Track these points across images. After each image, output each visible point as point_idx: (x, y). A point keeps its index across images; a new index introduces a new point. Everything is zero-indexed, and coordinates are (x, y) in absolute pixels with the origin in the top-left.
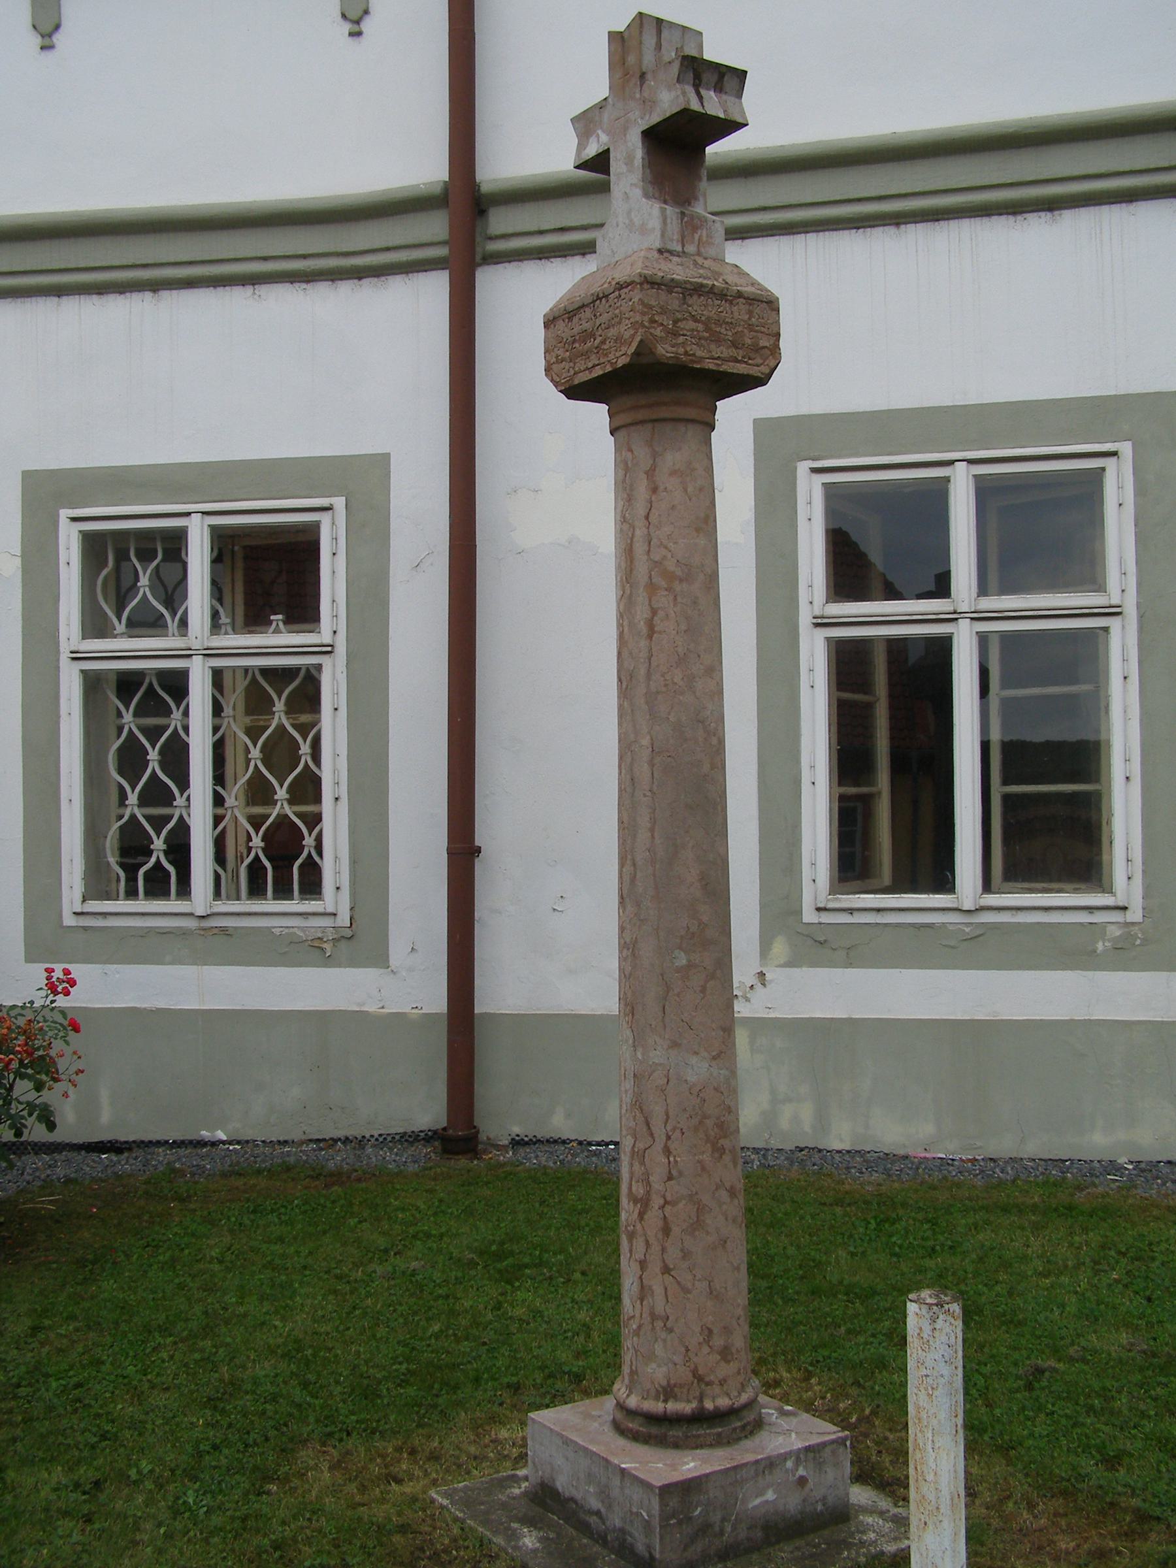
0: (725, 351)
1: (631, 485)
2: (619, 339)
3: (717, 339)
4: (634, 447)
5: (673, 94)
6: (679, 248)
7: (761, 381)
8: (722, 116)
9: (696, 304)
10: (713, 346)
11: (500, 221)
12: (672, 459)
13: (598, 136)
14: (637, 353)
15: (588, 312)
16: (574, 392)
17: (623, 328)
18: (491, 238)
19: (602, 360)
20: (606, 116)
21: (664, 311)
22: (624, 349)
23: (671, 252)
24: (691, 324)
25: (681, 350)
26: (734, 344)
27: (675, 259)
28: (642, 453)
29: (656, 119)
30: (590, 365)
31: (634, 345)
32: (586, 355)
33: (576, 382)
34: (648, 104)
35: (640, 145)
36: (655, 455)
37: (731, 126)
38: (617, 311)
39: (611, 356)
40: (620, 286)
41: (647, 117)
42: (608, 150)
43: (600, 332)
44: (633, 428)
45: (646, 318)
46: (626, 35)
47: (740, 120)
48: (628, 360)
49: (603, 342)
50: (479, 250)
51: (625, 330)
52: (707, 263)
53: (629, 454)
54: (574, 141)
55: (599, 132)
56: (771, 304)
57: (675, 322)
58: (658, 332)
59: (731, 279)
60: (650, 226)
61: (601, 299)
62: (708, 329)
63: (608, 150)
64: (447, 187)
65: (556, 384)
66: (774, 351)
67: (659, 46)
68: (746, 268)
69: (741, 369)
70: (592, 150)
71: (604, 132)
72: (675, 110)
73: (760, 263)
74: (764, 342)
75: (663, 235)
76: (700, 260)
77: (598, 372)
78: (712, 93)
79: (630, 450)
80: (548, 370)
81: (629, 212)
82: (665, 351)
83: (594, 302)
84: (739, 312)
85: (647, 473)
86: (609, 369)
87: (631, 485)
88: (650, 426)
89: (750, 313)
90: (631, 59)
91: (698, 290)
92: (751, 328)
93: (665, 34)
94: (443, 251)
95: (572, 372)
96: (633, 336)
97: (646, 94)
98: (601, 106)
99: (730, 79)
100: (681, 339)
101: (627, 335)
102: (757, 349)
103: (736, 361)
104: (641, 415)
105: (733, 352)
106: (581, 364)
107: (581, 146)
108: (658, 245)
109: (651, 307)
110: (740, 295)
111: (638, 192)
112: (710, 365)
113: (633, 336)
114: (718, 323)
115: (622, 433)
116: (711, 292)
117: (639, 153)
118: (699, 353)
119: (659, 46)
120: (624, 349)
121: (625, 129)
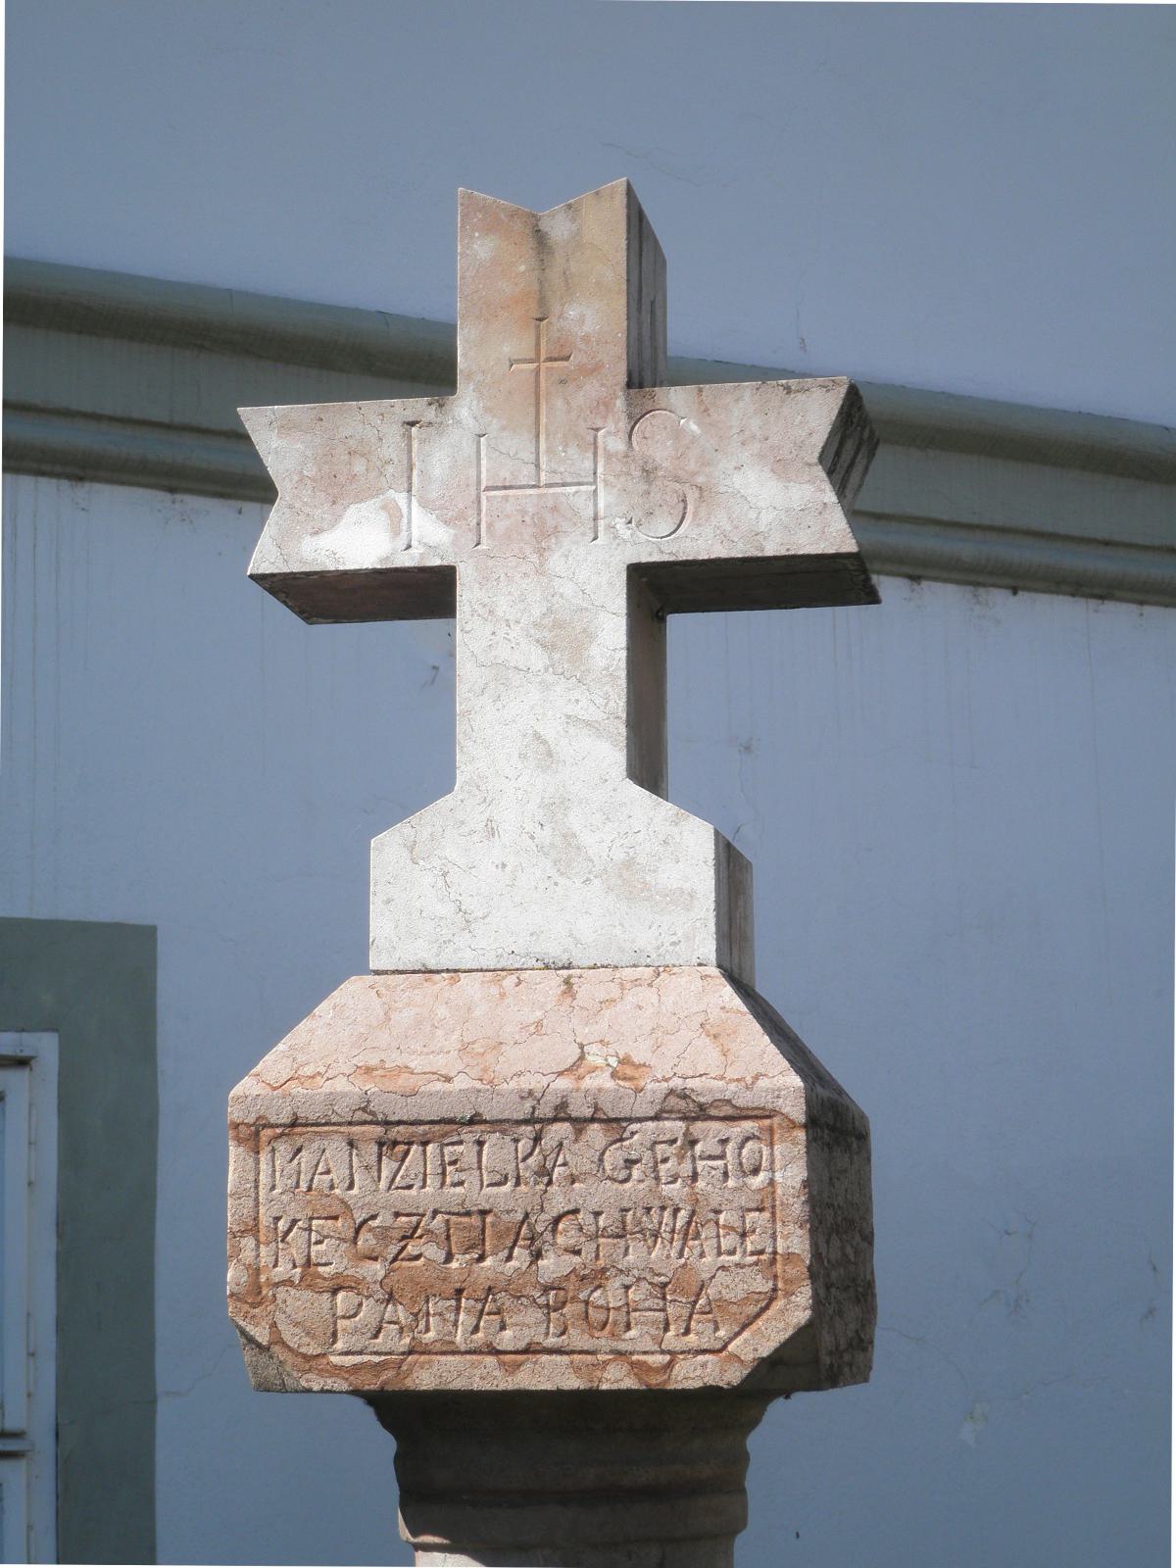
15: (497, 1152)
19: (577, 1338)
39: (636, 1337)
49: (596, 1278)
61: (580, 1124)
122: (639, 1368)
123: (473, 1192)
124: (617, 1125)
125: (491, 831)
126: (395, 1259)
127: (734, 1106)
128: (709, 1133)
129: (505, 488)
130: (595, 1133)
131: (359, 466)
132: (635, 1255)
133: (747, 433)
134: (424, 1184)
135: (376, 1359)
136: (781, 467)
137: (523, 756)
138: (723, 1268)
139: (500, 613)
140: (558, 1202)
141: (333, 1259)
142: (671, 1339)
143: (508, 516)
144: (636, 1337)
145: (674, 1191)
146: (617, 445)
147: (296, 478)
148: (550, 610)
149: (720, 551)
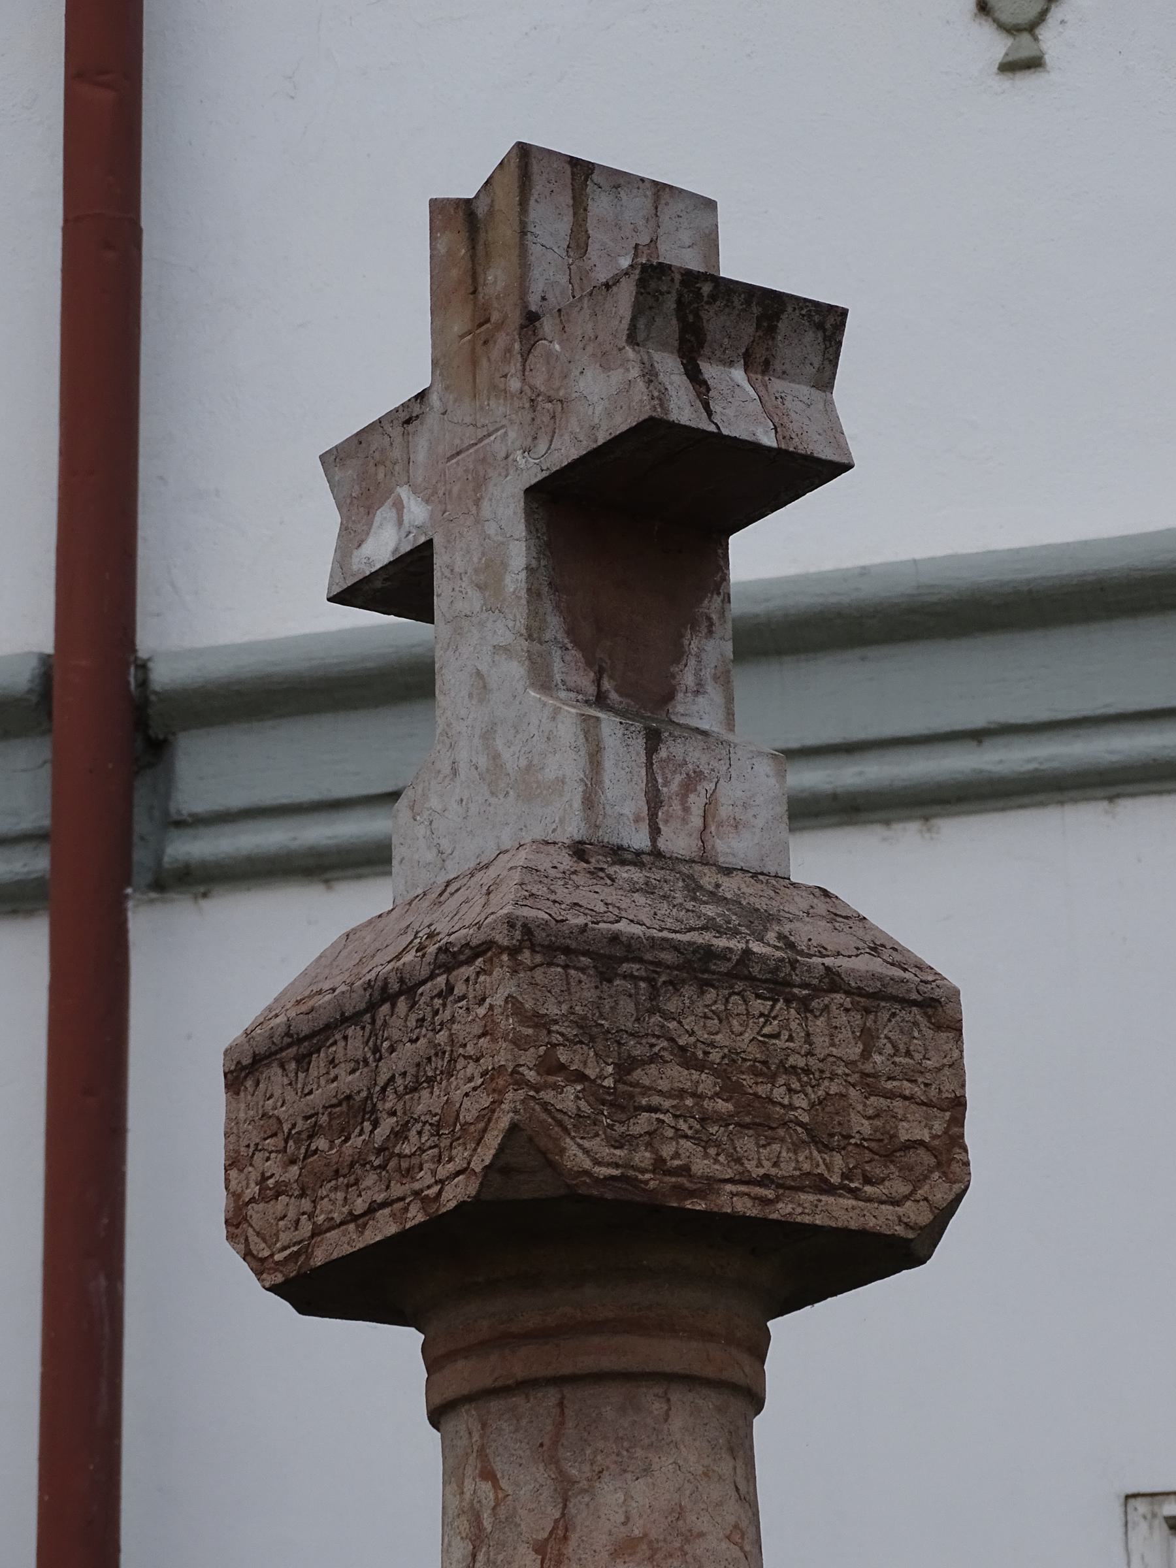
0: (790, 1161)
2: (446, 1125)
3: (760, 1120)
4: (499, 1466)
5: (617, 377)
6: (639, 839)
7: (905, 1251)
8: (768, 440)
9: (694, 1016)
10: (746, 1143)
11: (211, 771)
12: (621, 1503)
13: (399, 506)
15: (355, 1043)
16: (319, 1289)
17: (458, 1087)
18: (180, 824)
19: (397, 1190)
20: (423, 446)
21: (587, 1032)
22: (460, 1155)
23: (618, 854)
24: (676, 1075)
25: (643, 1157)
26: (816, 1137)
27: (625, 873)
28: (527, 1486)
29: (566, 450)
30: (360, 1206)
31: (493, 1140)
32: (345, 1174)
33: (319, 1257)
34: (545, 407)
35: (520, 529)
36: (565, 1490)
37: (796, 472)
38: (442, 1037)
39: (425, 1178)
40: (451, 958)
41: (542, 447)
42: (429, 543)
44: (495, 1405)
45: (529, 1057)
46: (481, 210)
47: (826, 453)
49: (399, 1134)
50: (141, 856)
51: (464, 1095)
52: (730, 886)
53: (486, 1486)
54: (334, 519)
55: (404, 492)
56: (933, 1008)
57: (625, 1067)
58: (568, 1099)
59: (807, 932)
60: (551, 772)
61: (392, 999)
62: (730, 1089)
63: (429, 543)
64: (48, 669)
65: (260, 1266)
66: (948, 1156)
67: (579, 242)
68: (854, 895)
69: (839, 1212)
70: (382, 547)
72: (622, 423)
73: (904, 891)
74: (912, 1129)
75: (589, 803)
76: (708, 879)
77: (384, 1227)
78: (738, 374)
79: (488, 1475)
80: (236, 1223)
81: (488, 735)
82: (585, 1155)
83: (372, 1007)
84: (834, 1034)
85: (540, 1548)
86: (416, 1216)
88: (551, 1397)
89: (868, 1038)
90: (497, 278)
91: (699, 967)
92: (869, 1084)
93: (600, 205)
94: (35, 863)
95: (306, 1228)
96: (487, 1115)
97: (539, 380)
98: (409, 415)
99: (798, 333)
100: (643, 1124)
102: (890, 1149)
103: (823, 1186)
104: (522, 1363)
105: (810, 1160)
106: (332, 1205)
107: (351, 537)
108: (574, 829)
109: (541, 1022)
110: (833, 981)
111: (515, 670)
112: (738, 1202)
113: (487, 1115)
114: (765, 1071)
115: (465, 1421)
116: (742, 973)
117: (518, 556)
118: (701, 1166)
119: (579, 242)
121: (480, 483)
122: (426, 1201)
123: (350, 1081)
124: (409, 989)
126: (305, 1158)
127: (471, 948)
129: (458, 454)
130: (402, 1004)
131: (381, 471)
133: (587, 337)
135: (295, 1249)
136: (605, 361)
137: (471, 696)
138: (467, 1095)
139: (457, 570)
143: (459, 479)
147: (348, 501)
148: (483, 554)
149: (574, 454)
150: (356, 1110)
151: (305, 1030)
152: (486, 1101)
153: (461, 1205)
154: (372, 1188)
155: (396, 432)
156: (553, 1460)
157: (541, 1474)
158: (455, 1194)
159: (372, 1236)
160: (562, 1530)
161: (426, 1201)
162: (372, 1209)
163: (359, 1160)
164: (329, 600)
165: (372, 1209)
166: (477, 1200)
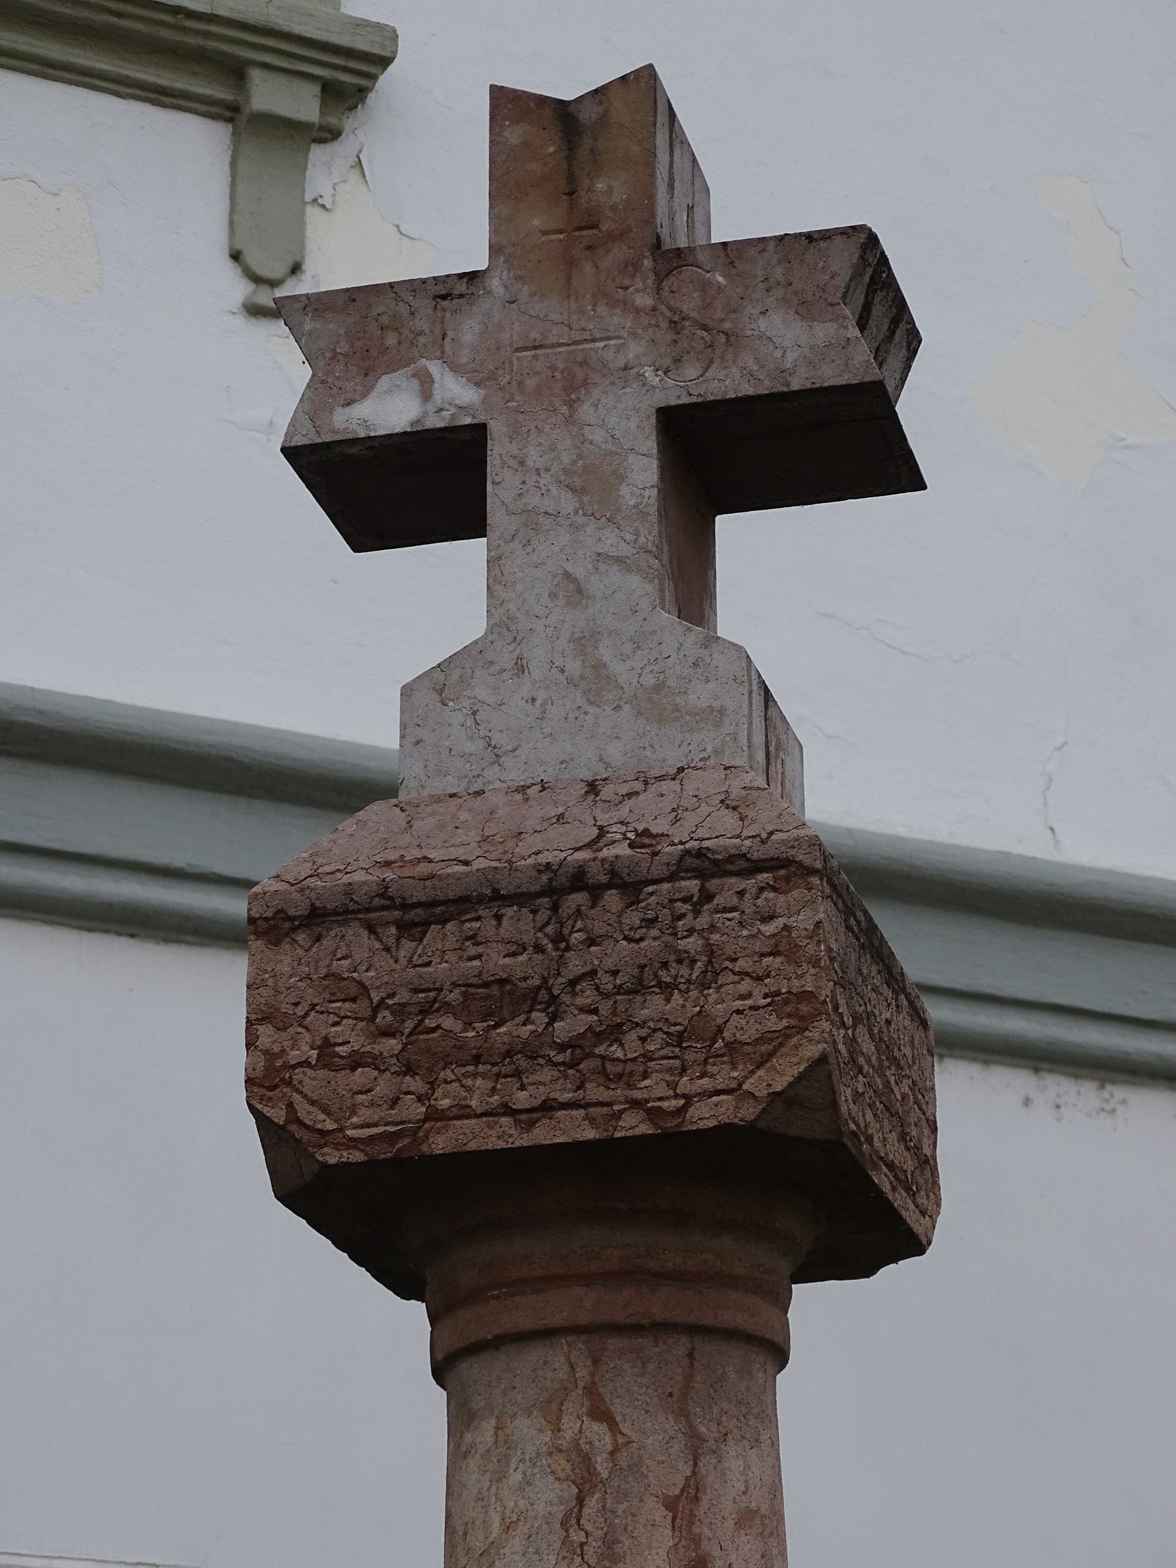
1: (610, 1543)
2: (696, 1039)
4: (618, 1409)
5: (824, 332)
14: (785, 1099)
15: (519, 924)
17: (719, 1005)
19: (595, 1092)
20: (468, 329)
22: (724, 1075)
29: (728, 381)
32: (515, 1060)
33: (440, 1144)
35: (650, 444)
36: (696, 1446)
40: (703, 864)
41: (691, 371)
43: (588, 996)
44: (614, 1343)
48: (749, 1112)
49: (614, 1033)
53: (598, 1430)
61: (596, 892)
71: (455, 368)
77: (572, 1129)
79: (601, 1414)
80: (266, 1083)
85: (671, 1504)
86: (633, 1125)
87: (610, 1543)
88: (681, 1345)
98: (452, 291)
101: (746, 1029)
104: (662, 1303)
107: (322, 394)
120: (724, 1075)
122: (654, 1114)
124: (631, 888)
125: (521, 668)
126: (411, 1034)
127: (748, 860)
128: (727, 889)
129: (535, 348)
130: (612, 899)
131: (391, 339)
132: (652, 1008)
133: (771, 280)
134: (444, 958)
135: (392, 1129)
136: (805, 309)
137: (553, 596)
138: (738, 1012)
139: (530, 463)
140: (575, 965)
141: (351, 1037)
142: (685, 1085)
143: (538, 373)
144: (653, 1087)
145: (692, 944)
146: (644, 300)
147: (328, 355)
148: (579, 457)
150: (497, 997)
151: (419, 894)
152: (774, 1023)
153: (724, 1129)
154: (545, 1083)
155: (424, 305)
156: (683, 1413)
157: (671, 1425)
158: (703, 1115)
159: (543, 1134)
160: (693, 1489)
161: (654, 1114)
162: (548, 1107)
163: (531, 1051)
164: (291, 453)
165: (548, 1107)
166: (752, 1124)
